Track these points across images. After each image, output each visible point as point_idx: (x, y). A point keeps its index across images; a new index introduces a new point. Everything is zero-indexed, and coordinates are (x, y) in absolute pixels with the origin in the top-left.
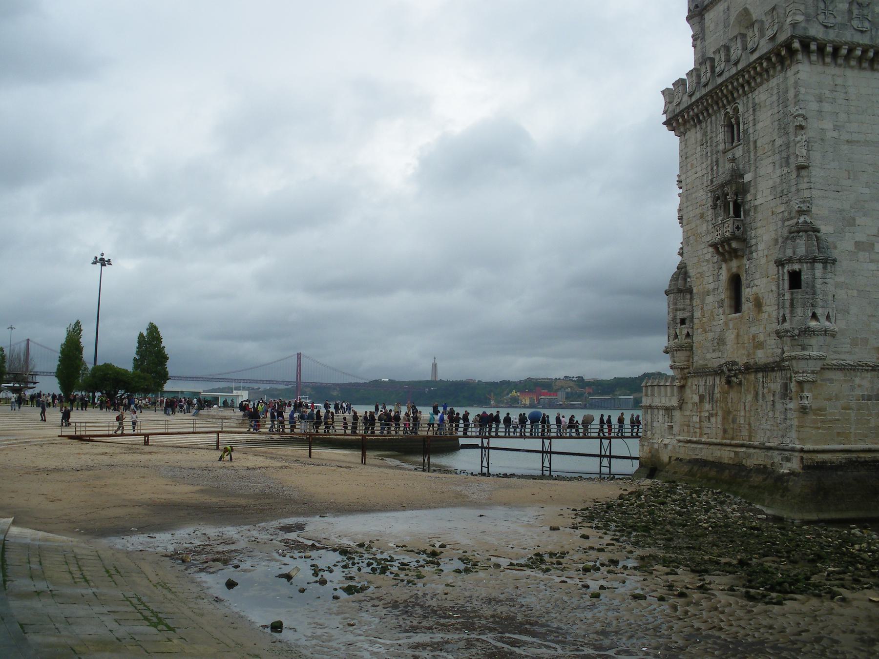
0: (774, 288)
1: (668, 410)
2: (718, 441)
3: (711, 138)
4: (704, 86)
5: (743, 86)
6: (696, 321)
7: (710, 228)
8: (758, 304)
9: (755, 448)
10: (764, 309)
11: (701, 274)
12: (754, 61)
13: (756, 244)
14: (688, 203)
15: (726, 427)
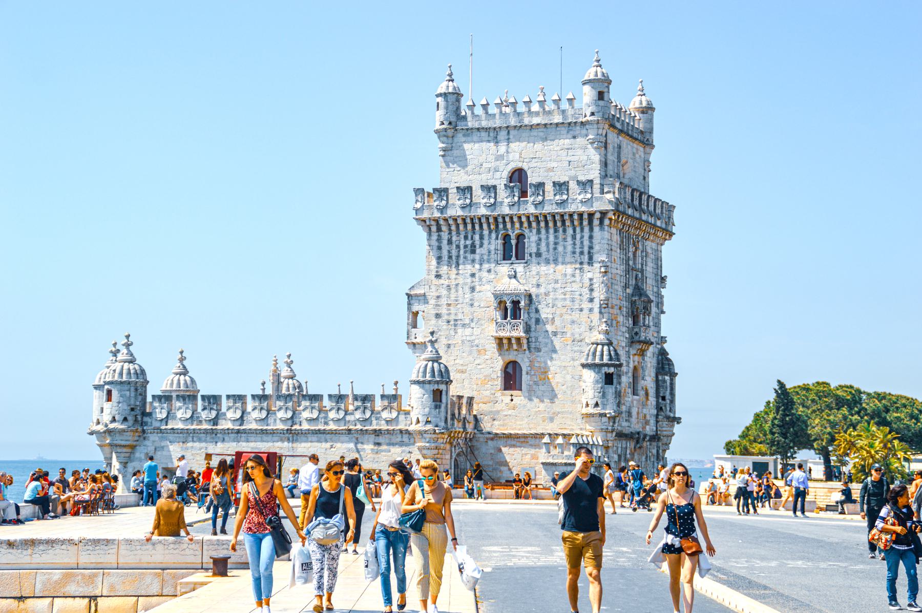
8: (647, 394)
10: (650, 398)
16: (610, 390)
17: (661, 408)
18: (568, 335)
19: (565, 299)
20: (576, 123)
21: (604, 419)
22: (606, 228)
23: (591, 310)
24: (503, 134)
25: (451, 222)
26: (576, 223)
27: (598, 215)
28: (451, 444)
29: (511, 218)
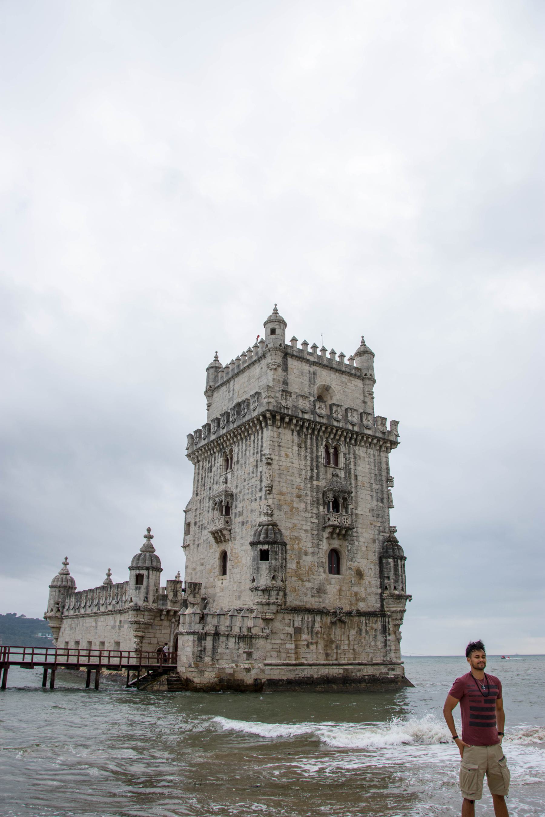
0: (373, 567)
1: (247, 638)
2: (325, 662)
3: (311, 449)
4: (319, 416)
5: (351, 439)
6: (288, 570)
7: (309, 508)
8: (360, 574)
9: (360, 664)
10: (365, 578)
11: (297, 538)
12: (371, 436)
13: (358, 537)
14: (281, 480)
15: (329, 652)
16: (264, 565)
17: (386, 588)
18: (249, 523)
19: (248, 493)
20: (261, 357)
21: (260, 593)
22: (269, 427)
23: (261, 498)
24: (232, 382)
25: (200, 452)
26: (254, 430)
27: (261, 418)
28: (170, 621)
29: (223, 438)
